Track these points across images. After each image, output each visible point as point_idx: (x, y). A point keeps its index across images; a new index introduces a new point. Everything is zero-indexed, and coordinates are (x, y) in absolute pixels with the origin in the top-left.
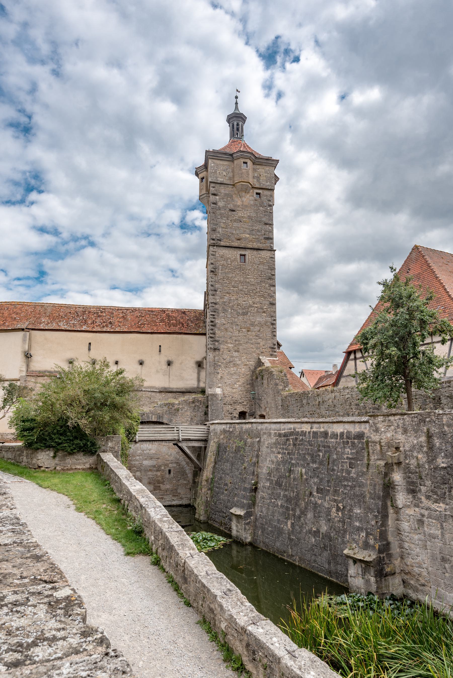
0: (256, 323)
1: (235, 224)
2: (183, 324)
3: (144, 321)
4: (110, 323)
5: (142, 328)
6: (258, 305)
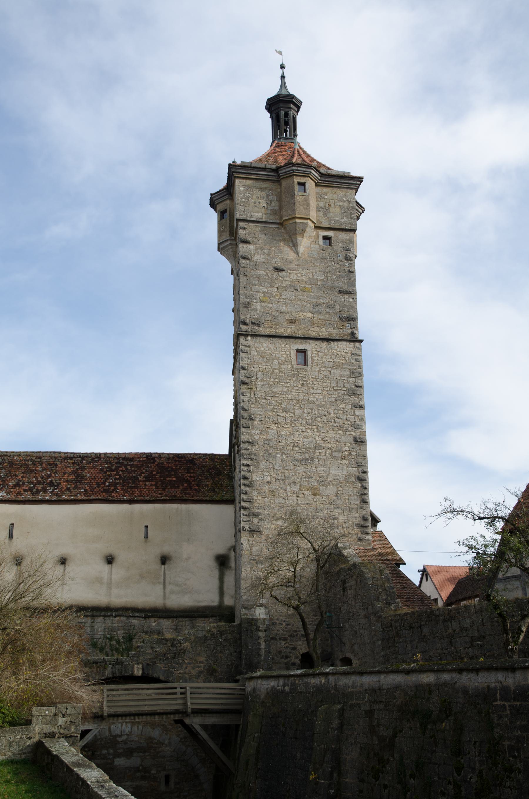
0: (330, 478)
1: (286, 295)
2: (189, 484)
3: (116, 479)
4: (51, 484)
5: (112, 492)
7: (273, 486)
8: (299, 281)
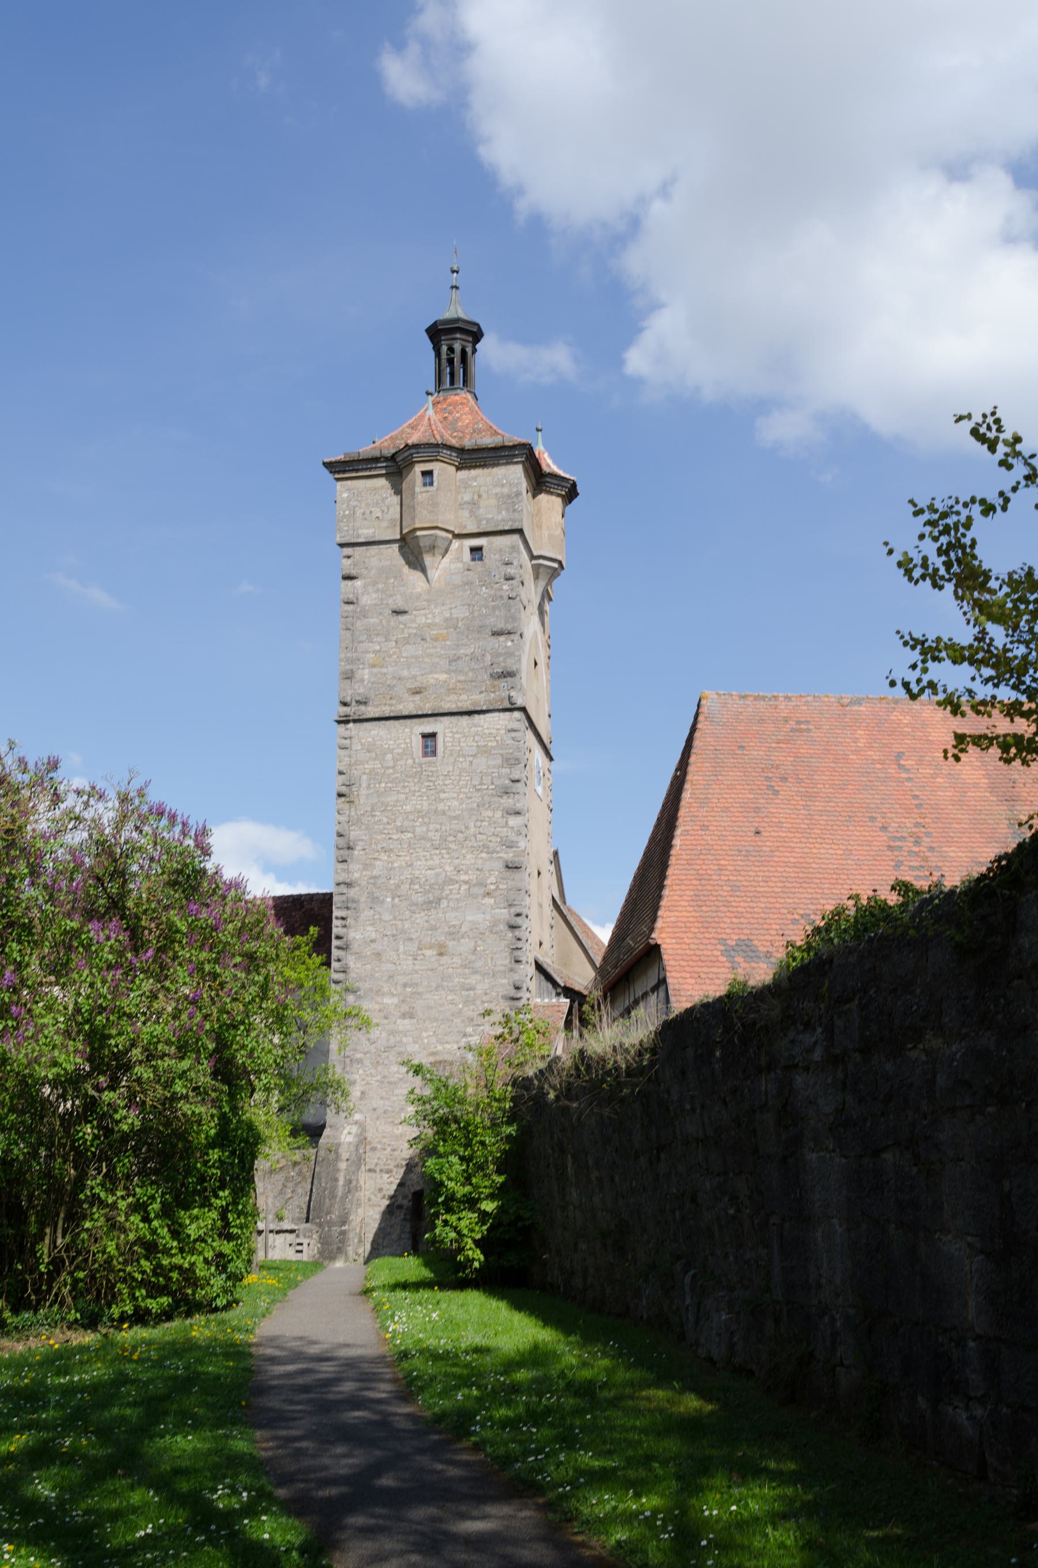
0: (463, 929)
1: (409, 650)
6: (472, 876)
7: (377, 947)
8: (429, 626)
